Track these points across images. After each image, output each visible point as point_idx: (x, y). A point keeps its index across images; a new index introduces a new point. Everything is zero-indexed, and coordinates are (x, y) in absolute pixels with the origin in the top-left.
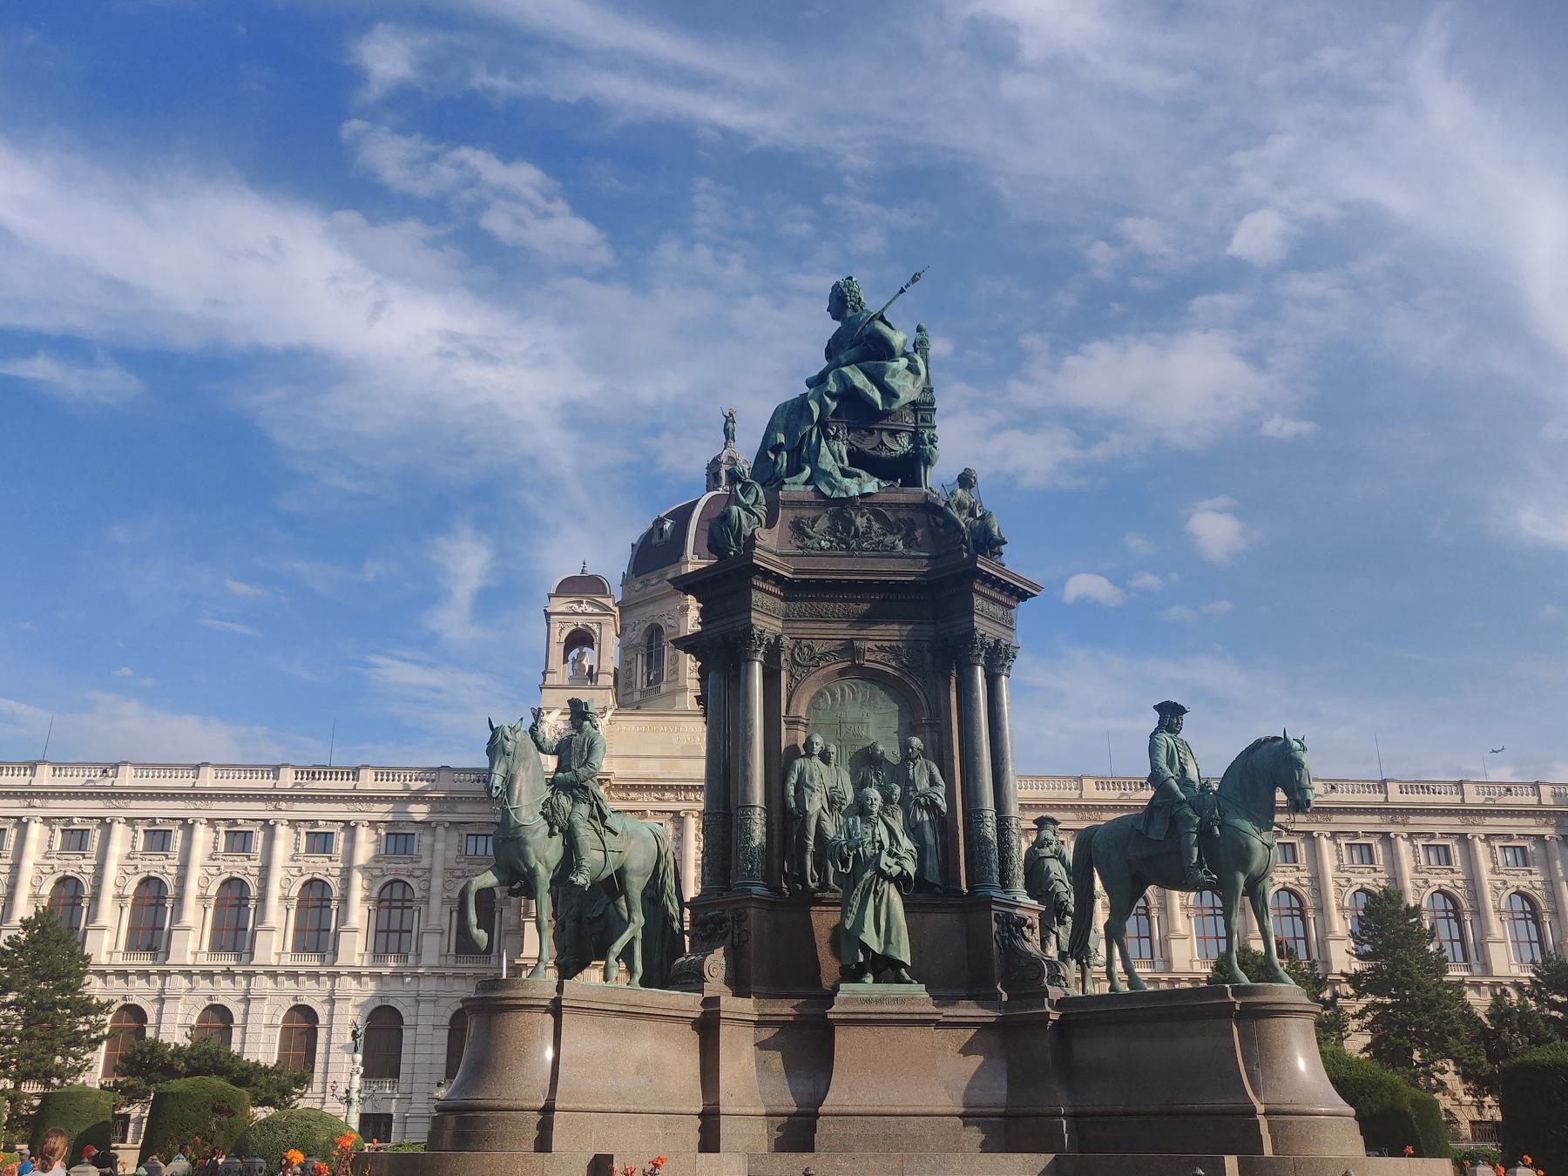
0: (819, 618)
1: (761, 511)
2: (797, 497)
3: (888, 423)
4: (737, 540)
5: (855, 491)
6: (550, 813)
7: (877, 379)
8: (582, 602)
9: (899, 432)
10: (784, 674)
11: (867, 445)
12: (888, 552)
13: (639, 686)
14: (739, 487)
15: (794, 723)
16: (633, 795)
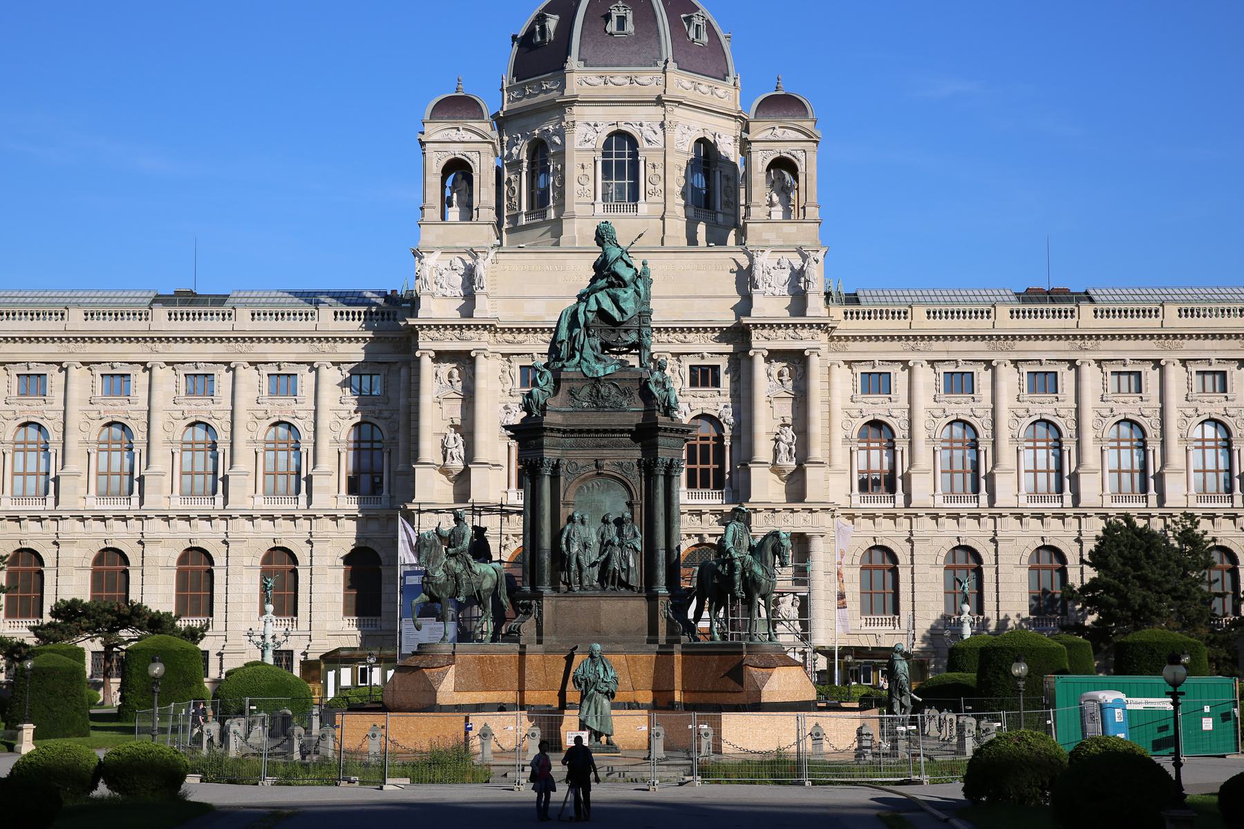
0: (580, 447)
1: (549, 388)
2: (570, 376)
3: (624, 327)
4: (537, 408)
5: (601, 373)
6: (447, 570)
7: (615, 300)
8: (458, 130)
9: (629, 330)
10: (562, 478)
11: (612, 338)
12: (618, 408)
13: (524, 209)
14: (538, 375)
15: (567, 504)
16: (521, 337)
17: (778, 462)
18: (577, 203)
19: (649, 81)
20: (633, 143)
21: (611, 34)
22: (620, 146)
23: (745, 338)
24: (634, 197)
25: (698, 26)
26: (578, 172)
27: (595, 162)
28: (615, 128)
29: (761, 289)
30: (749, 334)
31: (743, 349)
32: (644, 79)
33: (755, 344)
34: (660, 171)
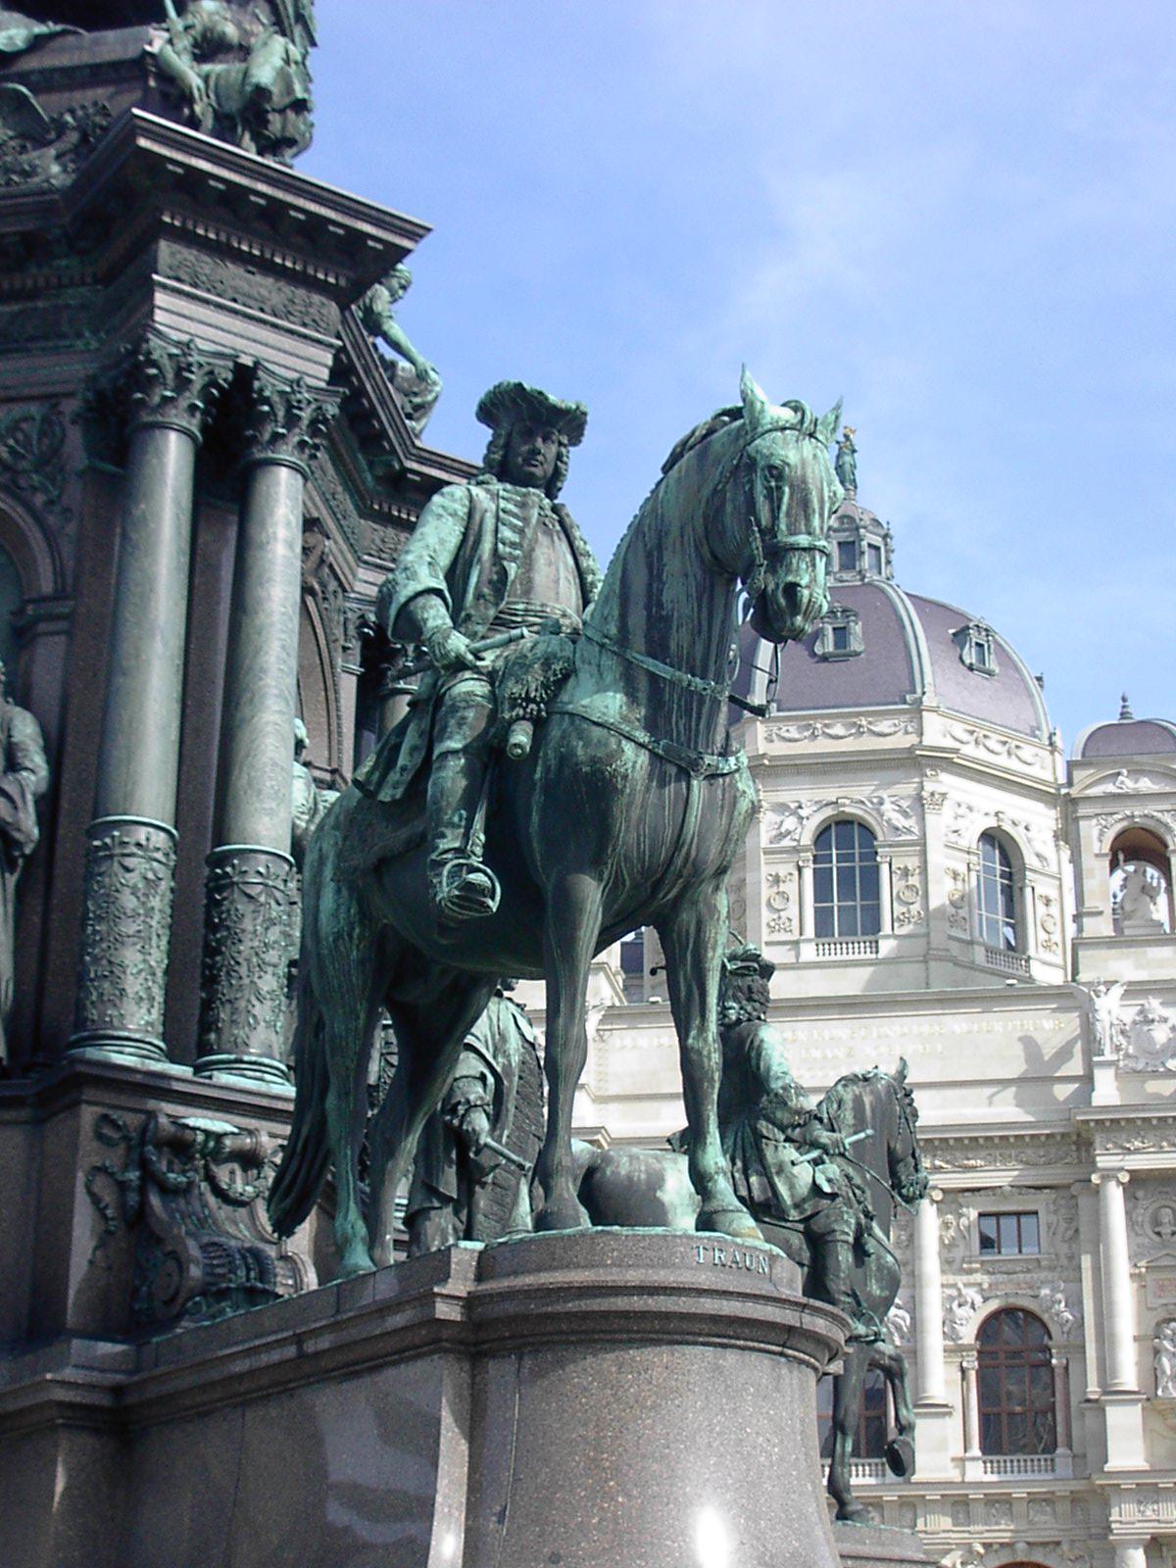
17: (1160, 1393)
18: (767, 944)
19: (891, 734)
20: (868, 832)
21: (825, 658)
22: (845, 843)
23: (1084, 1154)
24: (873, 926)
25: (978, 645)
26: (766, 891)
27: (800, 869)
28: (829, 812)
29: (1109, 1056)
30: (1090, 1144)
31: (1082, 1177)
32: (884, 726)
33: (1103, 1162)
34: (915, 880)
